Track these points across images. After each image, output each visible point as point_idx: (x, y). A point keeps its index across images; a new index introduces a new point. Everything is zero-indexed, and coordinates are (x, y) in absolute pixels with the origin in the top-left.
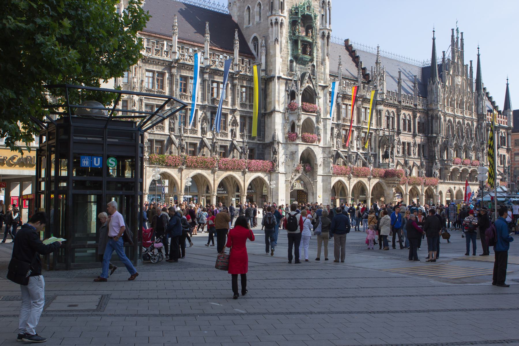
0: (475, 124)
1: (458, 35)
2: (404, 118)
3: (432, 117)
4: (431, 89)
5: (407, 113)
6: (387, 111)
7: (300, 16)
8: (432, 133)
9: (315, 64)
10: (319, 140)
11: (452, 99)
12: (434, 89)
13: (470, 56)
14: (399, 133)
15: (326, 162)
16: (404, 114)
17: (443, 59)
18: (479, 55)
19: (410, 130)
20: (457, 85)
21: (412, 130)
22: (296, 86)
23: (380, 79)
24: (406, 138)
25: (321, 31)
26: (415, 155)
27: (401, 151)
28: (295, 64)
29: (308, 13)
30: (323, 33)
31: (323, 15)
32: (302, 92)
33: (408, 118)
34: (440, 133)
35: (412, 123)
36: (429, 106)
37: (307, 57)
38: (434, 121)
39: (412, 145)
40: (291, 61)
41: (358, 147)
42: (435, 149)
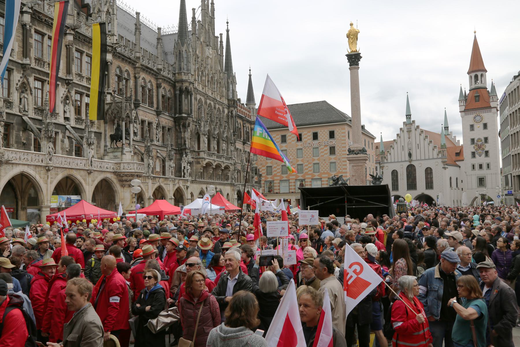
0: (226, 111)
2: (143, 84)
3: (181, 90)
4: (180, 53)
5: (148, 78)
6: (119, 67)
11: (202, 73)
12: (184, 53)
13: (219, 29)
14: (137, 106)
16: (143, 79)
17: (194, 18)
18: (228, 31)
19: (151, 104)
20: (208, 57)
21: (155, 106)
24: (146, 114)
26: (158, 141)
27: (139, 133)
33: (149, 86)
35: (155, 94)
36: (177, 75)
38: (183, 96)
39: (154, 126)
41: (67, 115)
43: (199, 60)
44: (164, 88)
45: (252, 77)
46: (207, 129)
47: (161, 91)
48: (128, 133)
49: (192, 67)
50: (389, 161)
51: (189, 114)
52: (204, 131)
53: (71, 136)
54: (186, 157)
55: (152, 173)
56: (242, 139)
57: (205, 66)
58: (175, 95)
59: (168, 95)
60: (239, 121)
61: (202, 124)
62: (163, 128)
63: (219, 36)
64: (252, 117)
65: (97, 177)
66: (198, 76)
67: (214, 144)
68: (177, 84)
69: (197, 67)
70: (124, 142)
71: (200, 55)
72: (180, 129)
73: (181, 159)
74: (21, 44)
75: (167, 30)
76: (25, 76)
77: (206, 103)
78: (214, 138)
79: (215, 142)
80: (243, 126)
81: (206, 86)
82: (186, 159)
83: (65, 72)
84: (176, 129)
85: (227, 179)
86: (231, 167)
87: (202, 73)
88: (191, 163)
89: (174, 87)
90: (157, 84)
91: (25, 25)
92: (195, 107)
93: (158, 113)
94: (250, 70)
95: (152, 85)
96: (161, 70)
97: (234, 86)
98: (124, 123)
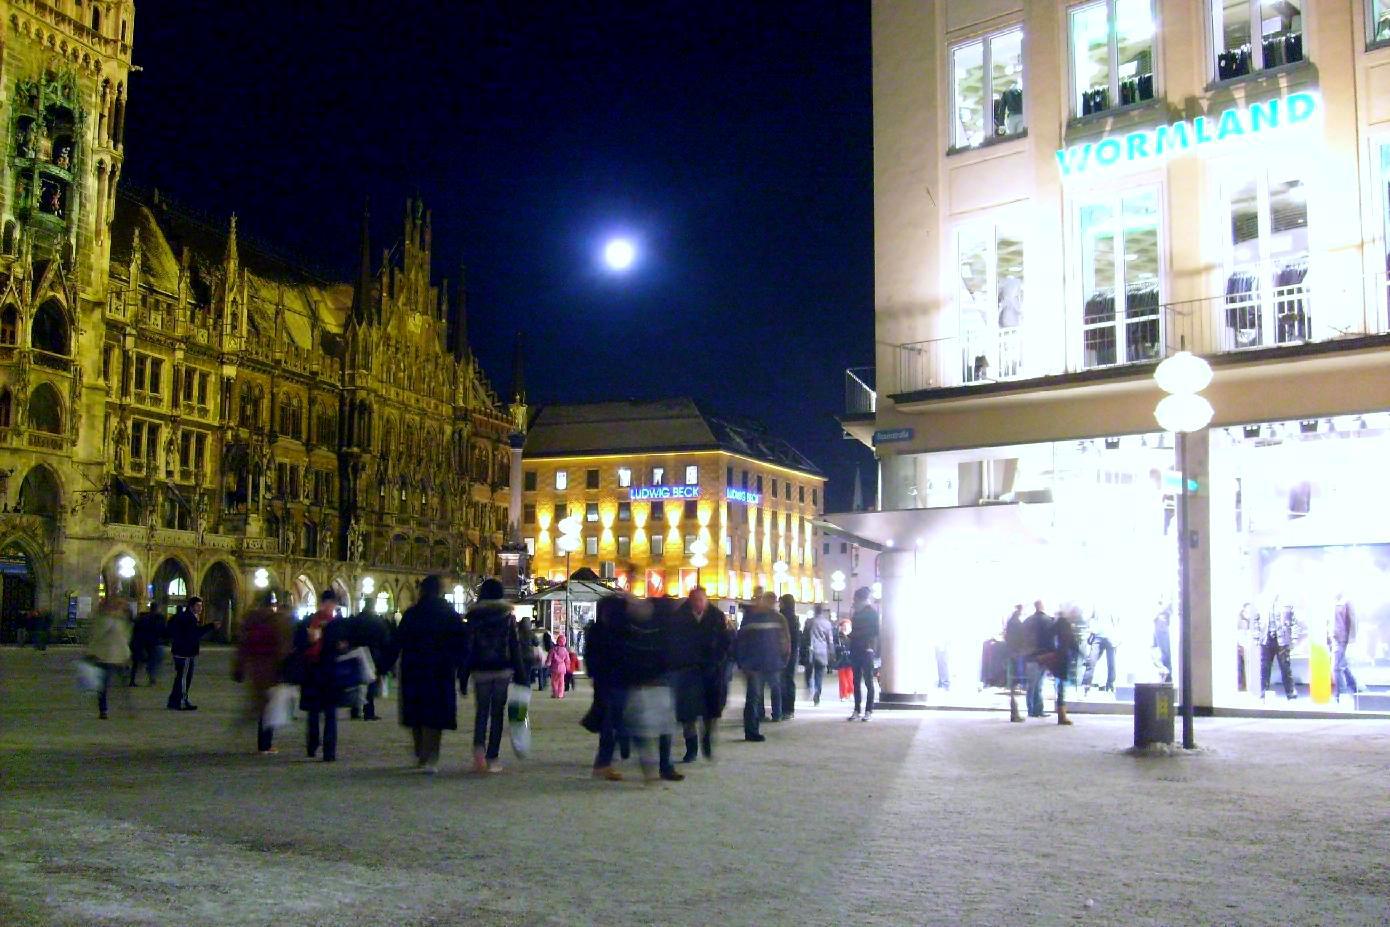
0: (448, 429)
3: (352, 404)
7: (41, 108)
8: (349, 445)
9: (73, 241)
10: (74, 444)
11: (398, 366)
15: (89, 503)
21: (304, 436)
22: (21, 292)
23: (234, 301)
25: (96, 158)
28: (17, 234)
29: (65, 105)
30: (101, 162)
31: (102, 116)
32: (34, 311)
33: (295, 402)
37: (52, 219)
38: (356, 415)
40: (9, 227)
41: (171, 468)
42: (355, 484)
43: (393, 342)
44: (323, 403)
46: (397, 474)
47: (317, 409)
48: (256, 488)
53: (175, 498)
55: (292, 553)
59: (330, 412)
62: (317, 473)
65: (208, 560)
70: (250, 507)
74: (121, 378)
76: (123, 420)
80: (494, 455)
83: (171, 405)
86: (451, 541)
87: (398, 366)
88: (366, 537)
90: (309, 398)
91: (128, 351)
92: (377, 433)
93: (309, 447)
95: (300, 401)
96: (316, 374)
98: (251, 477)
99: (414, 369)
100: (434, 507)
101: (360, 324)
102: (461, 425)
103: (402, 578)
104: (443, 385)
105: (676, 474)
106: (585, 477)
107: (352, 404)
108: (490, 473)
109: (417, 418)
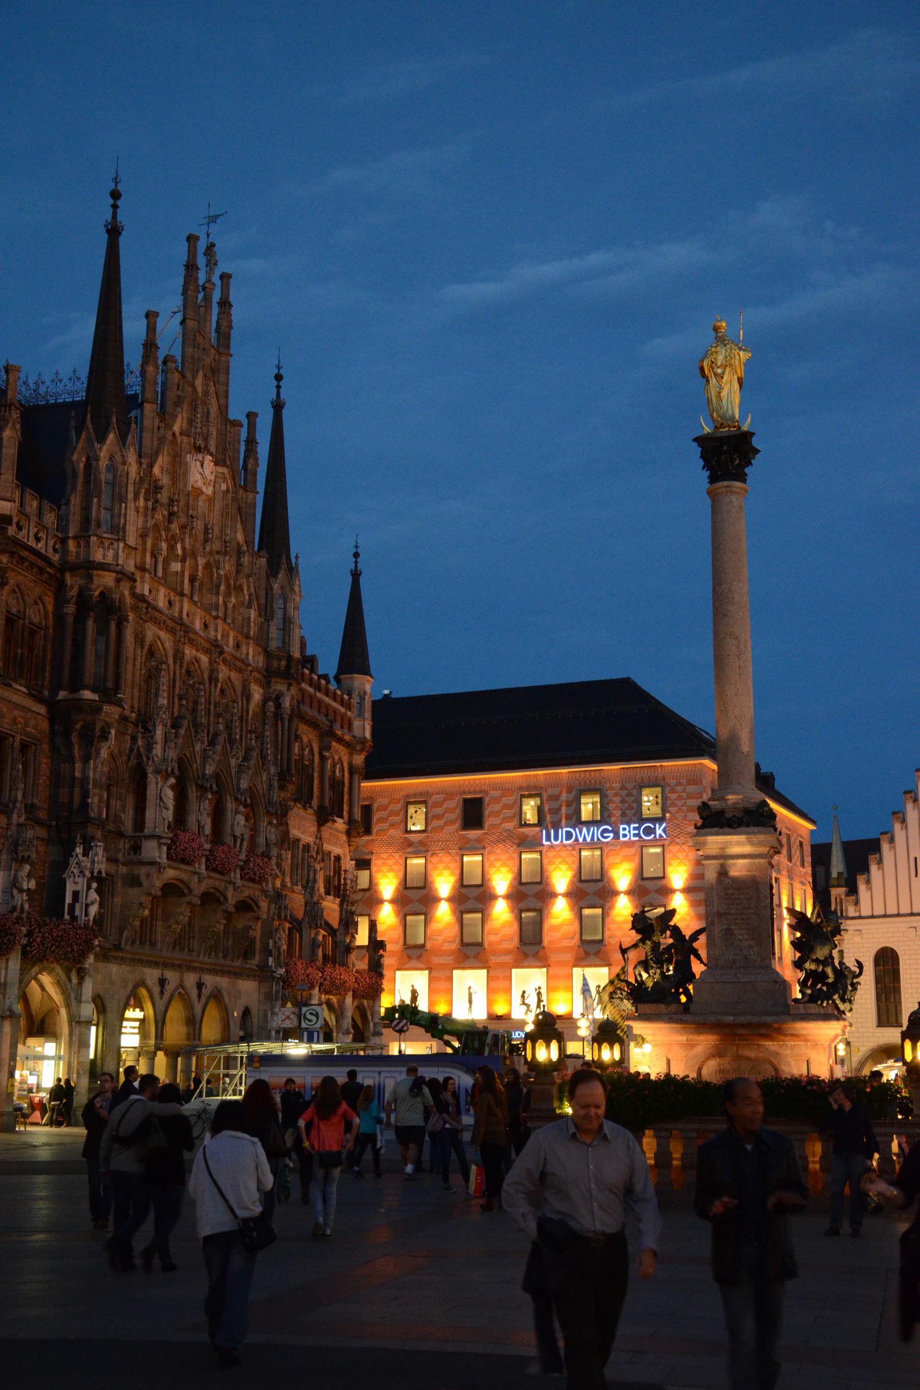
0: (257, 694)
1: (210, 273)
8: (76, 685)
11: (171, 548)
12: (103, 463)
13: (247, 394)
17: (150, 346)
18: (278, 407)
20: (198, 492)
34: (117, 688)
38: (90, 623)
42: (84, 771)
43: (163, 497)
45: (362, 580)
46: (172, 754)
49: (134, 522)
50: (865, 910)
51: (110, 694)
52: (164, 759)
54: (85, 854)
56: (315, 803)
57: (183, 520)
58: (59, 616)
59: (34, 616)
60: (307, 734)
61: (159, 732)
63: (245, 422)
64: (356, 723)
66: (154, 556)
67: (200, 816)
68: (69, 579)
69: (150, 523)
71: (165, 481)
72: (69, 746)
73: (65, 865)
75: (52, 389)
77: (178, 655)
78: (202, 789)
79: (206, 806)
80: (323, 758)
81: (182, 594)
82: (86, 863)
84: (54, 748)
85: (247, 954)
86: (264, 905)
87: (171, 548)
88: (103, 883)
89: (60, 589)
92: (133, 669)
94: (356, 555)
97: (291, 606)
99: (201, 561)
100: (238, 833)
101: (102, 439)
102: (279, 686)
103: (172, 976)
104: (249, 606)
105: (623, 801)
106: (458, 812)
107: (83, 599)
108: (315, 790)
109: (204, 659)
